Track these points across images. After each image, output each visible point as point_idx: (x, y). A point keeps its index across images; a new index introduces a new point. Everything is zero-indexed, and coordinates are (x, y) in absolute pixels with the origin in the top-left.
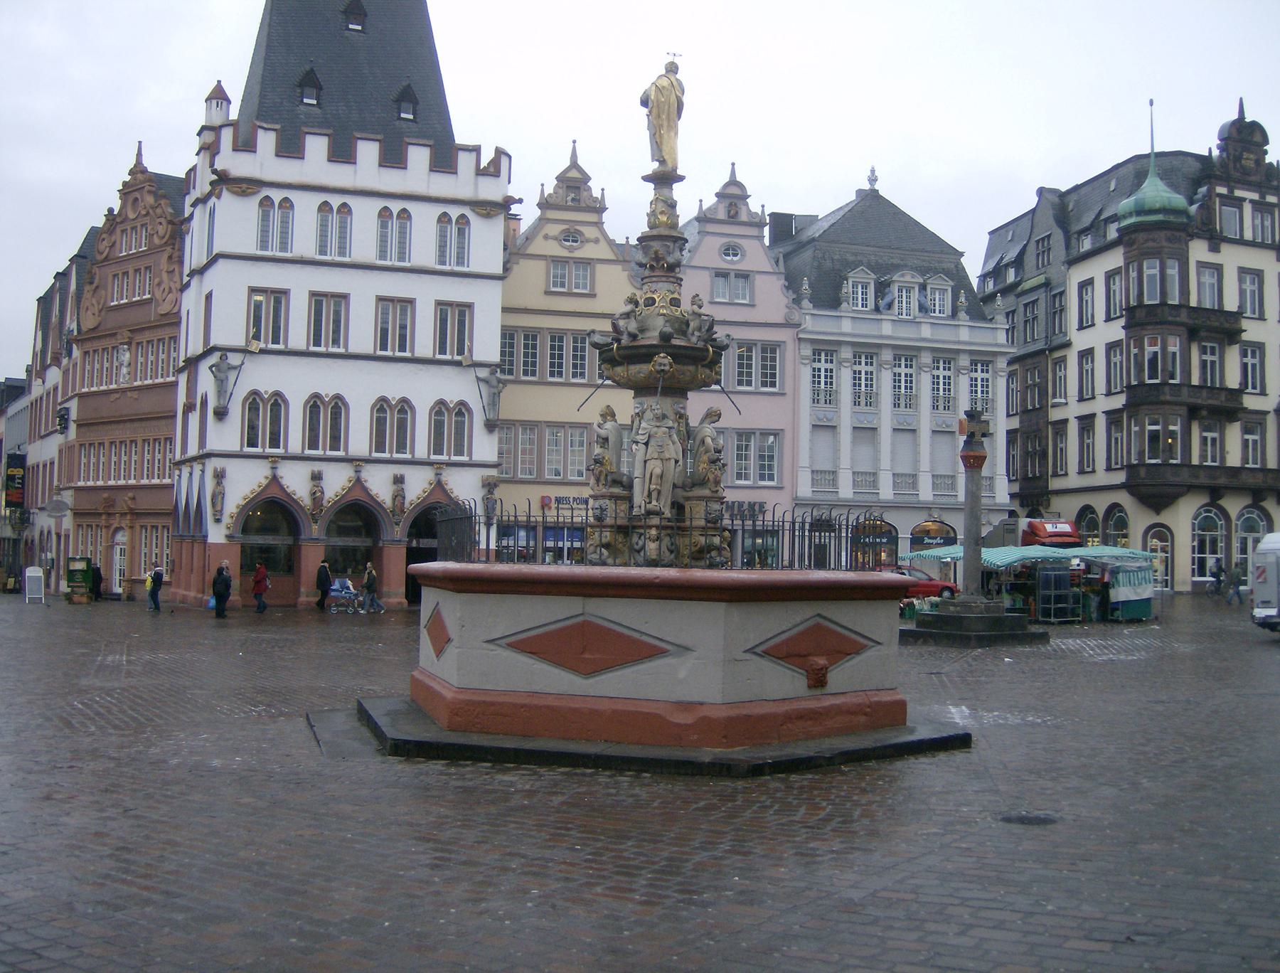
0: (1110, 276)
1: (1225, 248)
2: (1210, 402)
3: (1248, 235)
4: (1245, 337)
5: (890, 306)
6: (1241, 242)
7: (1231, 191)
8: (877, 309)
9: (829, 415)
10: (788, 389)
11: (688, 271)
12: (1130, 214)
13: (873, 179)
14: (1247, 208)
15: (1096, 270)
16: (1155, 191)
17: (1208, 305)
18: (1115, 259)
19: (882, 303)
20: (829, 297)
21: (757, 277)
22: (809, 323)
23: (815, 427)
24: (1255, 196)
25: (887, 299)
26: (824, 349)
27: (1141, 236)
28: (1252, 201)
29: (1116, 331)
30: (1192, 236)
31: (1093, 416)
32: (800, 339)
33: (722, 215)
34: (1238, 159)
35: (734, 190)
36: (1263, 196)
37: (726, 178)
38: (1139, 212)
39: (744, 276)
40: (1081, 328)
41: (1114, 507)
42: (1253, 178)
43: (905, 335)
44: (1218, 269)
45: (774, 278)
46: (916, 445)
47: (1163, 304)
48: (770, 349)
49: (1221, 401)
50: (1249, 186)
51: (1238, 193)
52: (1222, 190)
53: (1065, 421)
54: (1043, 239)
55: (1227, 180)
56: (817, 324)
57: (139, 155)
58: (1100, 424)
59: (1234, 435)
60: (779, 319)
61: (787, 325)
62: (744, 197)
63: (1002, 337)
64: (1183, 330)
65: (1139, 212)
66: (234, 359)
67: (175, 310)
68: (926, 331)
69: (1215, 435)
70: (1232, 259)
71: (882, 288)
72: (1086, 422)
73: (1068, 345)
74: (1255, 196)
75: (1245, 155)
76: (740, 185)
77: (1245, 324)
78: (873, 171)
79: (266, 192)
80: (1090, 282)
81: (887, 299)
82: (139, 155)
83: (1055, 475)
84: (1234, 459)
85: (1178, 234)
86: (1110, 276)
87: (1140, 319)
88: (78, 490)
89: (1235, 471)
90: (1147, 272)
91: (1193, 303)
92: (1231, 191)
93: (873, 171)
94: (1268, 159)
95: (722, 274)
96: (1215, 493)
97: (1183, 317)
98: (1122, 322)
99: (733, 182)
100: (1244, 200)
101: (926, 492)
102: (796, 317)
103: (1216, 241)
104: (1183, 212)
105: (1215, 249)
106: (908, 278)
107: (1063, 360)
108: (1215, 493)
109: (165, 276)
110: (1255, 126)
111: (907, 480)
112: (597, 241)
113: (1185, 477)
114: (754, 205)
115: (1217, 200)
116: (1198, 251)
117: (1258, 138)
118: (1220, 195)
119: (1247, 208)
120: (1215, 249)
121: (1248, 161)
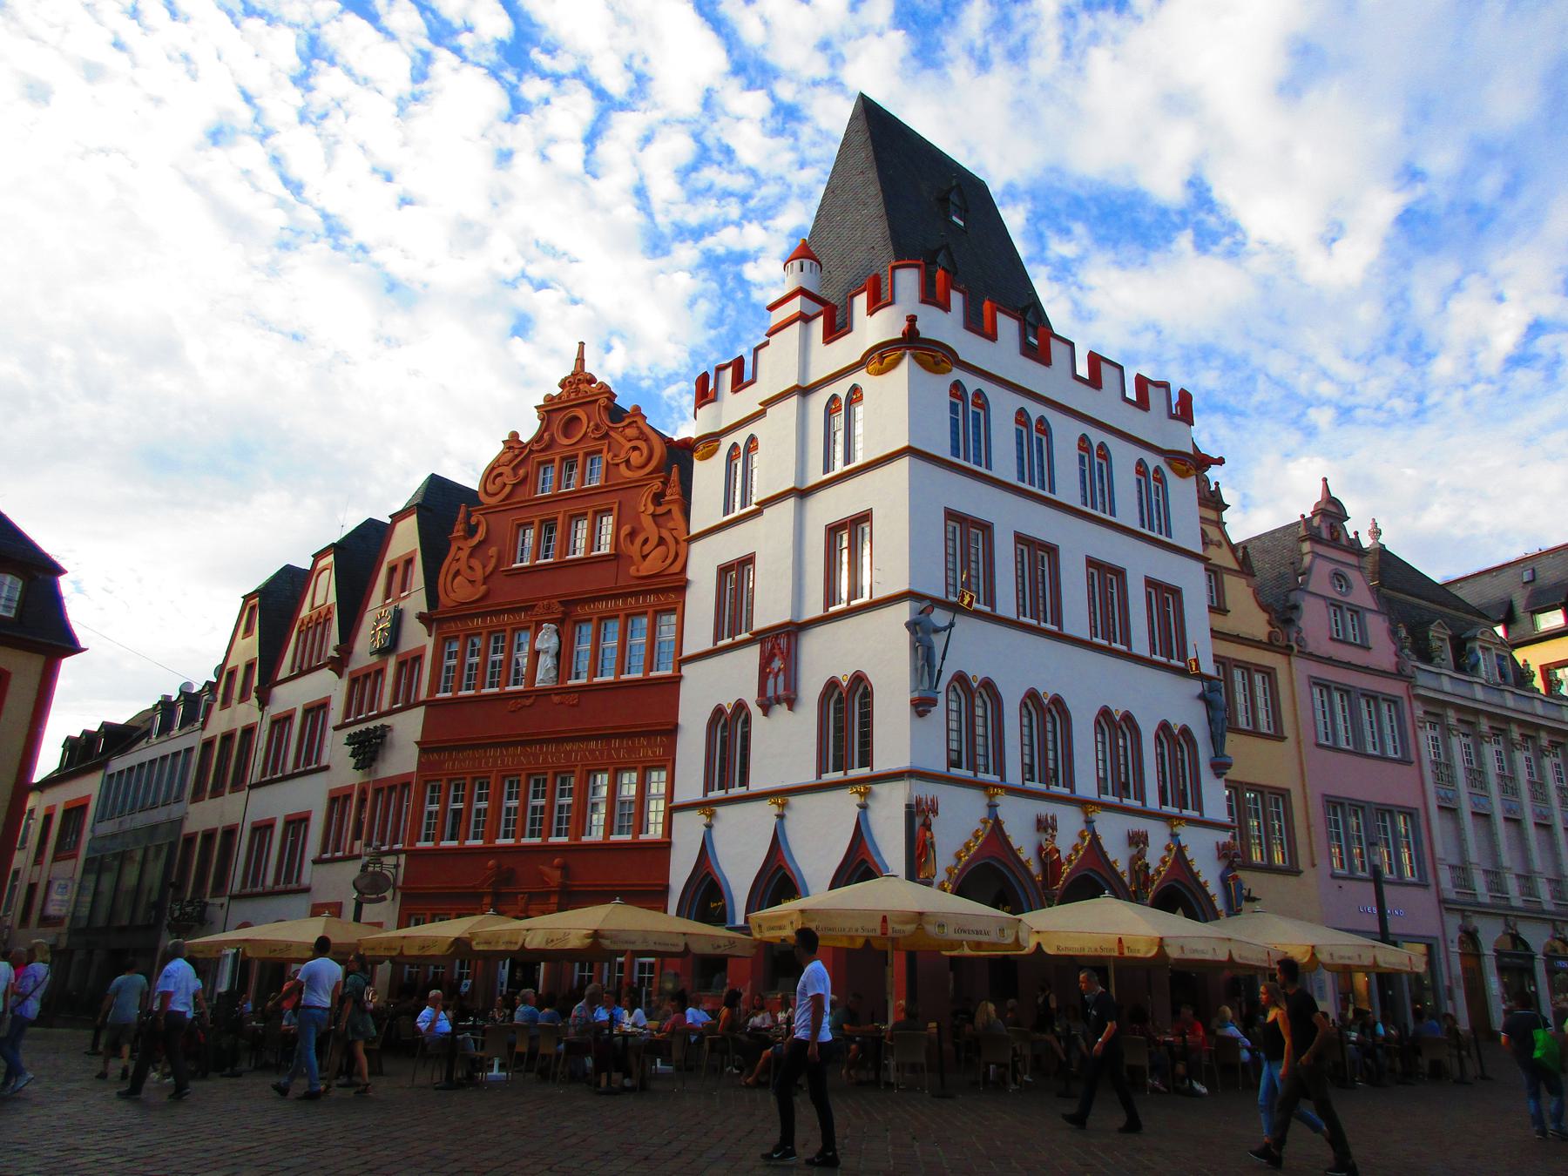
11: (1307, 598)
26: (1436, 709)
32: (1418, 697)
33: (1325, 534)
35: (1332, 508)
37: (1318, 497)
39: (1356, 611)
57: (580, 360)
61: (1398, 674)
66: (940, 617)
67: (676, 568)
79: (957, 374)
82: (580, 360)
88: (414, 855)
95: (1336, 606)
109: (647, 521)
112: (1219, 545)
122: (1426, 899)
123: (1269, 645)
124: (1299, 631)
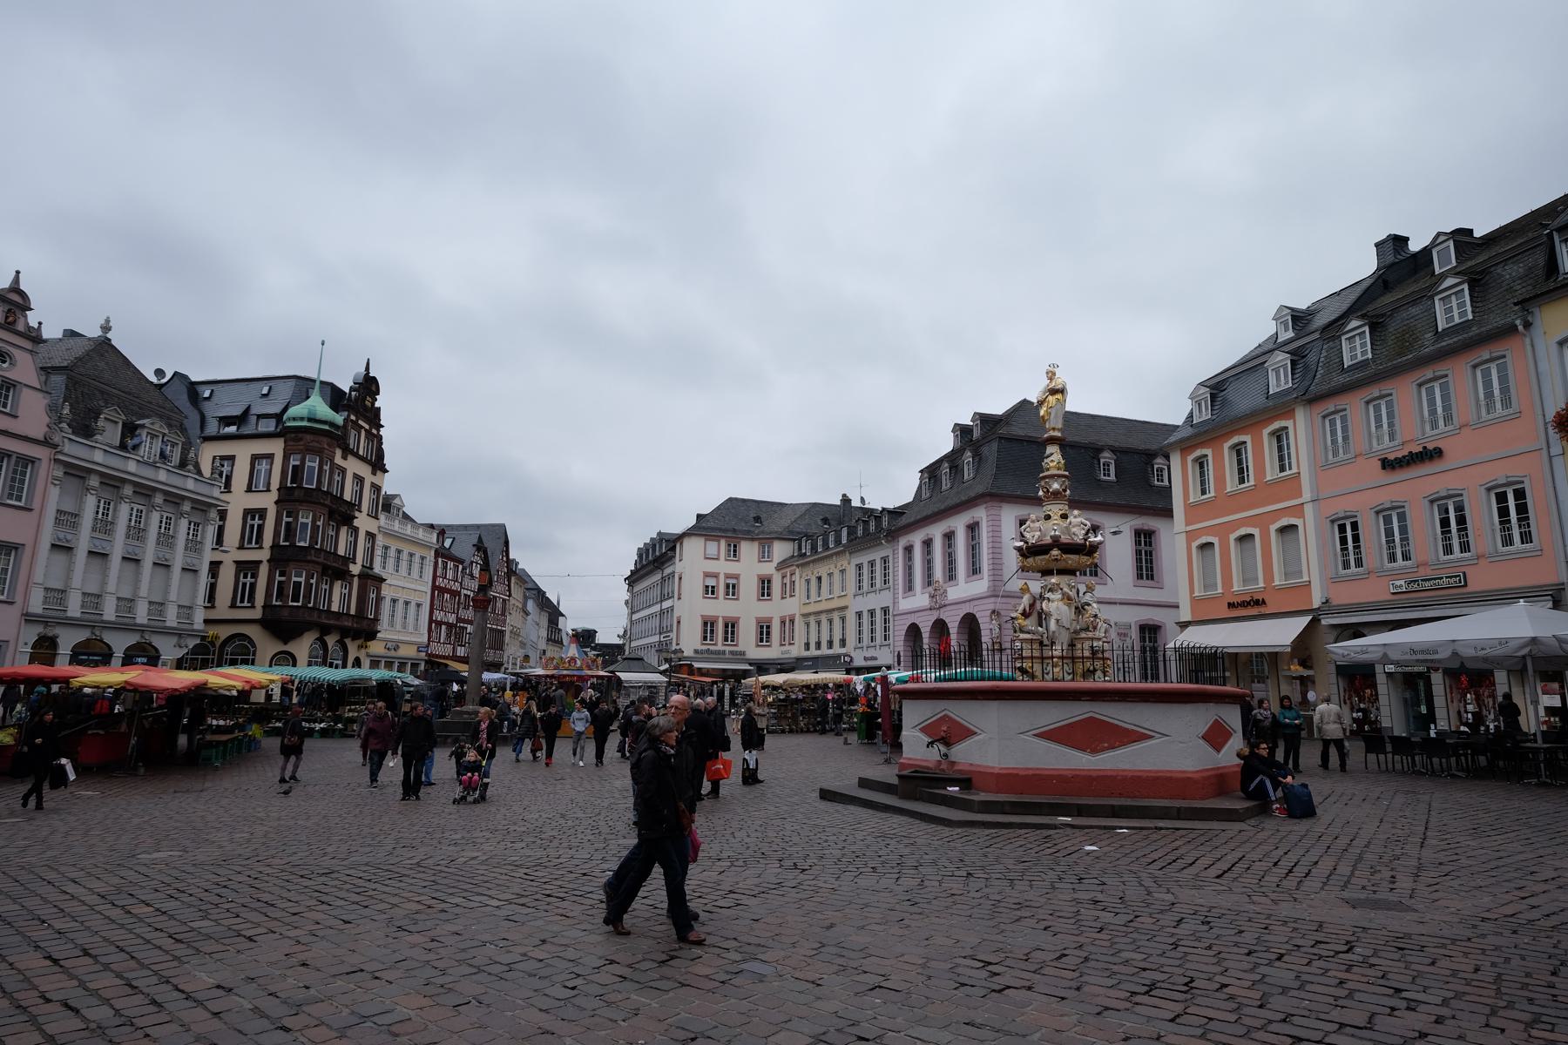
0: (255, 458)
1: (350, 457)
4: (356, 523)
5: (136, 447)
6: (356, 455)
8: (123, 446)
9: (69, 537)
10: (36, 505)
12: (302, 419)
13: (106, 328)
15: (243, 452)
16: (317, 405)
18: (276, 447)
19: (130, 443)
20: (85, 429)
21: (25, 390)
22: (68, 448)
23: (90, 552)
25: (136, 441)
26: (76, 473)
27: (309, 437)
29: (267, 501)
35: (15, 298)
38: (310, 420)
44: (343, 471)
45: (40, 395)
46: (138, 574)
47: (318, 489)
48: (27, 461)
56: (75, 450)
60: (39, 434)
61: (46, 442)
62: (25, 306)
64: (326, 511)
65: (310, 420)
68: (162, 476)
70: (353, 466)
71: (130, 430)
72: (215, 567)
76: (22, 294)
78: (108, 321)
80: (232, 458)
81: (136, 441)
84: (335, 608)
86: (255, 458)
87: (290, 498)
89: (338, 615)
90: (308, 464)
93: (108, 321)
94: (377, 405)
96: (325, 630)
98: (274, 495)
99: (15, 288)
101: (142, 615)
102: (57, 439)
103: (347, 452)
105: (344, 458)
106: (156, 427)
110: (374, 378)
111: (127, 603)
113: (315, 617)
114: (33, 319)
120: (344, 458)
122: (14, 613)
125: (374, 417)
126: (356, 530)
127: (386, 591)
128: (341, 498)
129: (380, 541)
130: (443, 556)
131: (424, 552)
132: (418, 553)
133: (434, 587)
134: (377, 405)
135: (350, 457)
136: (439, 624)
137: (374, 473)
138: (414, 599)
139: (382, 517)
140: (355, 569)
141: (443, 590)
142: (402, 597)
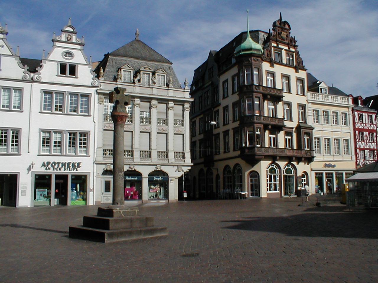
1: (275, 65)
2: (272, 123)
3: (284, 62)
4: (284, 99)
5: (139, 81)
6: (281, 64)
7: (278, 45)
10: (92, 114)
14: (284, 53)
17: (270, 86)
19: (136, 80)
24: (287, 48)
28: (285, 50)
30: (263, 60)
31: (228, 131)
34: (280, 34)
36: (289, 48)
40: (224, 98)
41: (237, 165)
42: (285, 41)
43: (146, 92)
44: (273, 74)
49: (276, 122)
50: (285, 44)
51: (280, 46)
52: (274, 44)
53: (219, 134)
54: (211, 69)
55: (276, 41)
58: (231, 133)
59: (281, 136)
61: (92, 86)
63: (188, 95)
68: (155, 91)
69: (274, 136)
70: (279, 70)
72: (226, 133)
73: (219, 105)
74: (287, 48)
75: (283, 32)
77: (284, 94)
83: (216, 154)
85: (258, 58)
86: (233, 78)
91: (265, 85)
92: (278, 45)
97: (261, 89)
100: (282, 49)
102: (97, 84)
103: (272, 63)
104: (259, 50)
105: (272, 66)
107: (218, 111)
108: (274, 159)
110: (285, 23)
115: (273, 48)
116: (266, 66)
117: (287, 27)
118: (273, 46)
119: (284, 53)
120: (272, 66)
121: (284, 35)
123: (23, 80)
124: (40, 74)
125: (292, 43)
126: (289, 104)
127: (315, 134)
128: (274, 88)
129: (310, 108)
130: (357, 111)
131: (345, 110)
132: (340, 110)
133: (355, 129)
134: (291, 35)
135: (275, 65)
136: (363, 150)
137: (297, 71)
138: (342, 137)
139: (309, 95)
140: (294, 124)
141: (361, 131)
142: (333, 136)
